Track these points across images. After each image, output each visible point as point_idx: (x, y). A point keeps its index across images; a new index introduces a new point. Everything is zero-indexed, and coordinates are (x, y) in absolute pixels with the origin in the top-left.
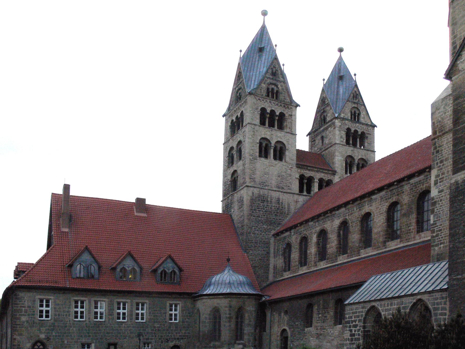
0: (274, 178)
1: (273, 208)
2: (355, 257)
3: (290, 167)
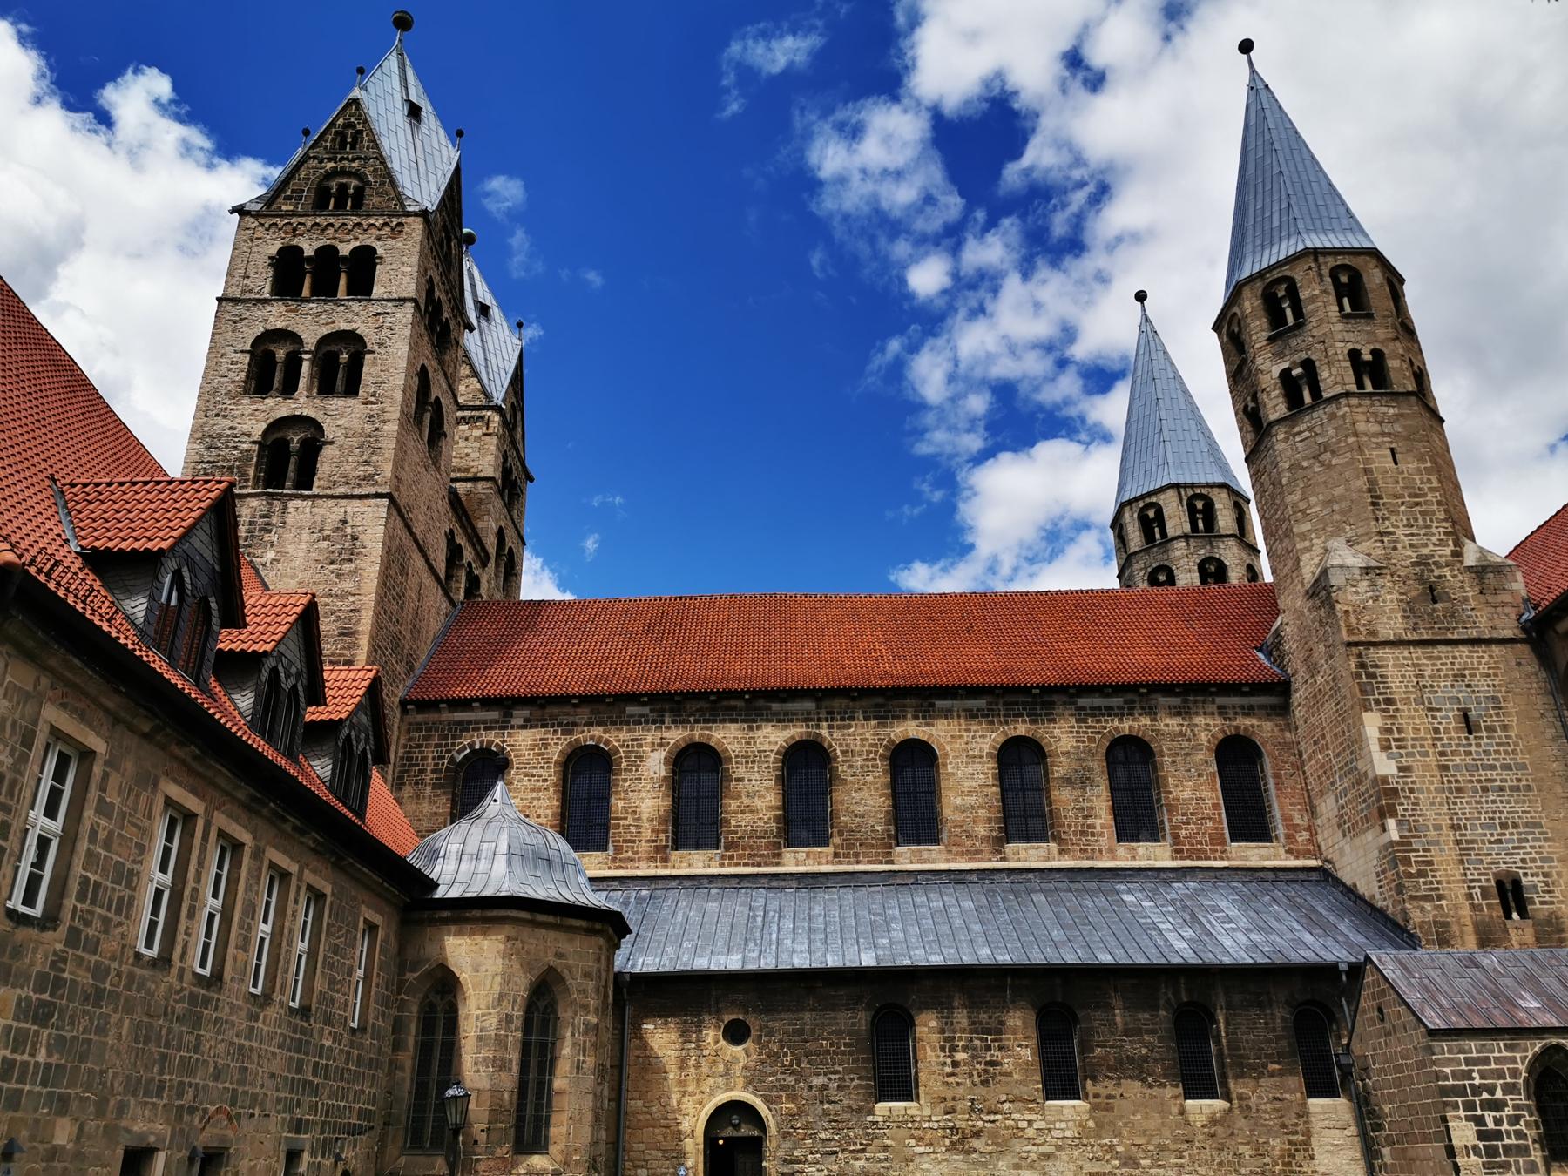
2: (869, 862)
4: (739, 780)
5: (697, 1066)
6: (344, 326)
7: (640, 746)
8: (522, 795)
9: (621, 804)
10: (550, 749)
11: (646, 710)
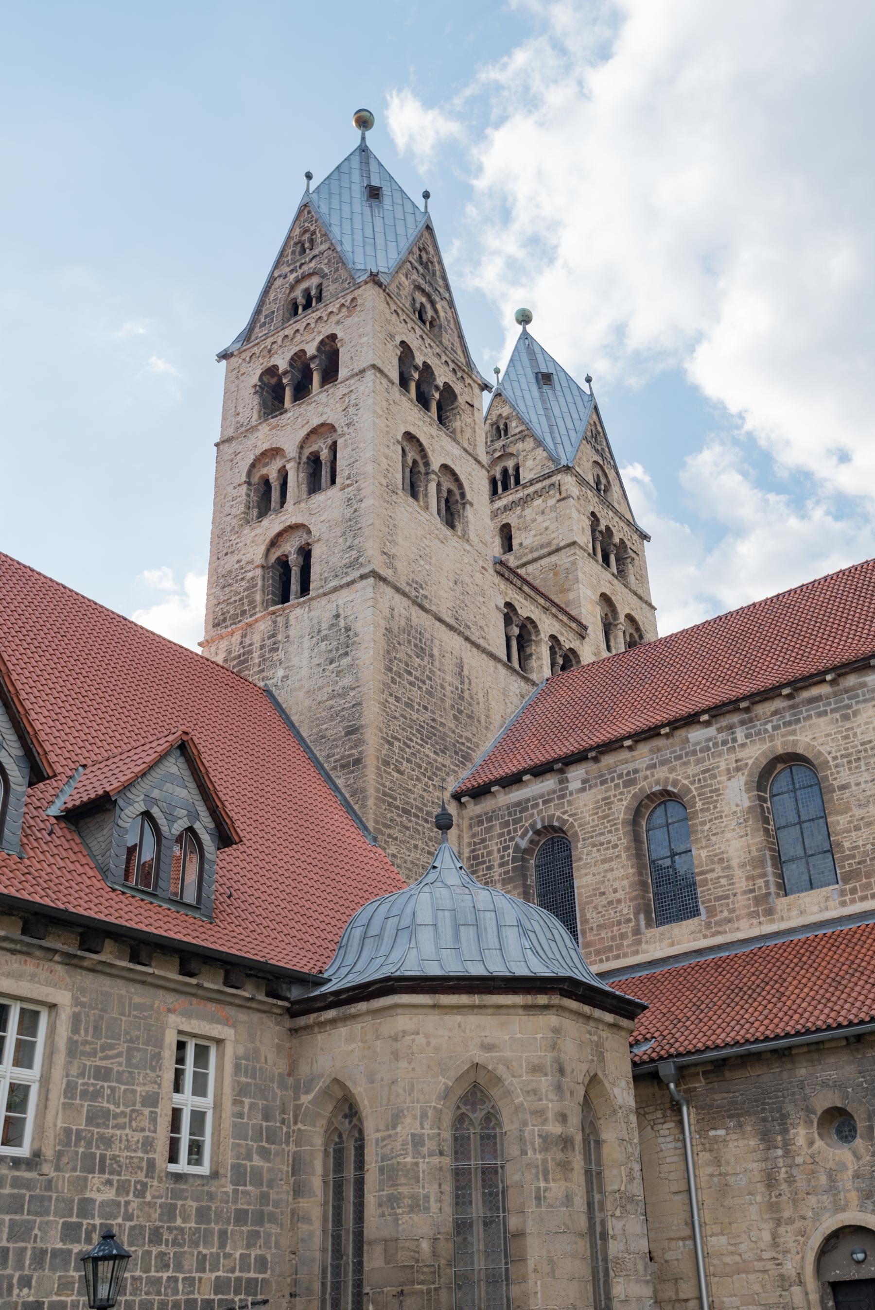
1: (449, 688)
4: (843, 787)
5: (791, 1180)
6: (315, 422)
7: (714, 777)
8: (593, 869)
9: (704, 853)
10: (615, 808)
11: (711, 731)
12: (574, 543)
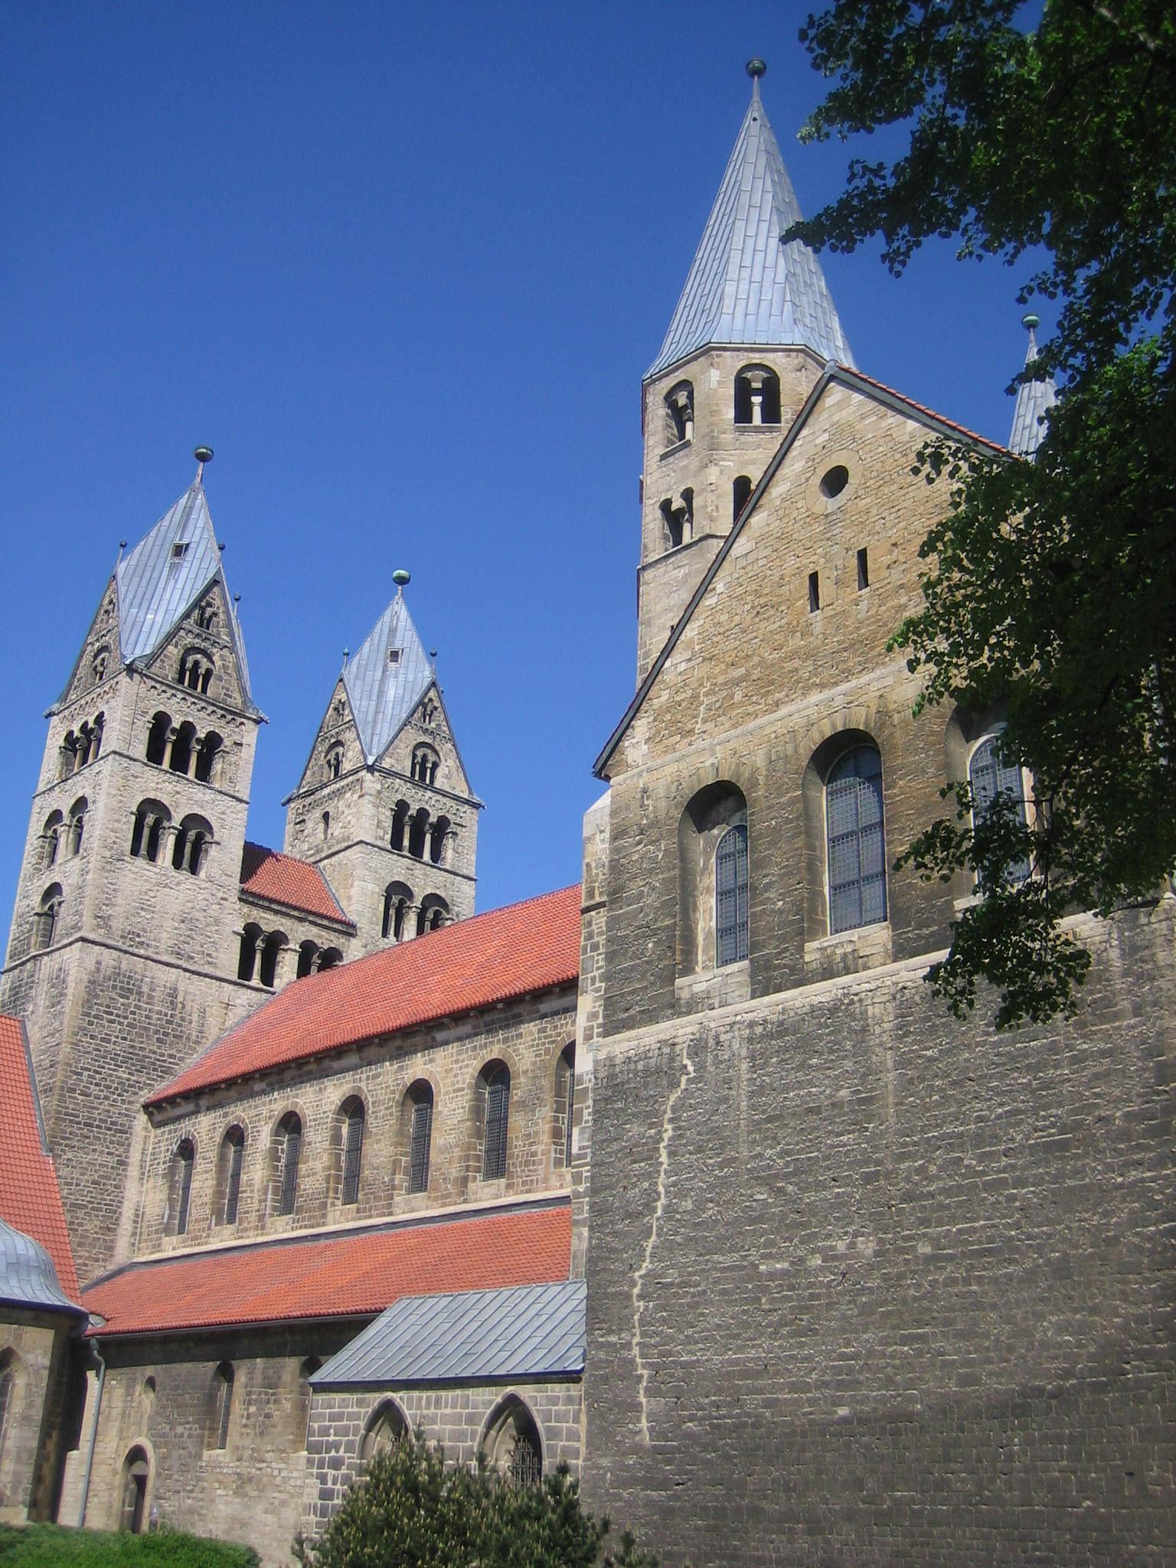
0: (169, 924)
3: (220, 894)
12: (361, 842)
